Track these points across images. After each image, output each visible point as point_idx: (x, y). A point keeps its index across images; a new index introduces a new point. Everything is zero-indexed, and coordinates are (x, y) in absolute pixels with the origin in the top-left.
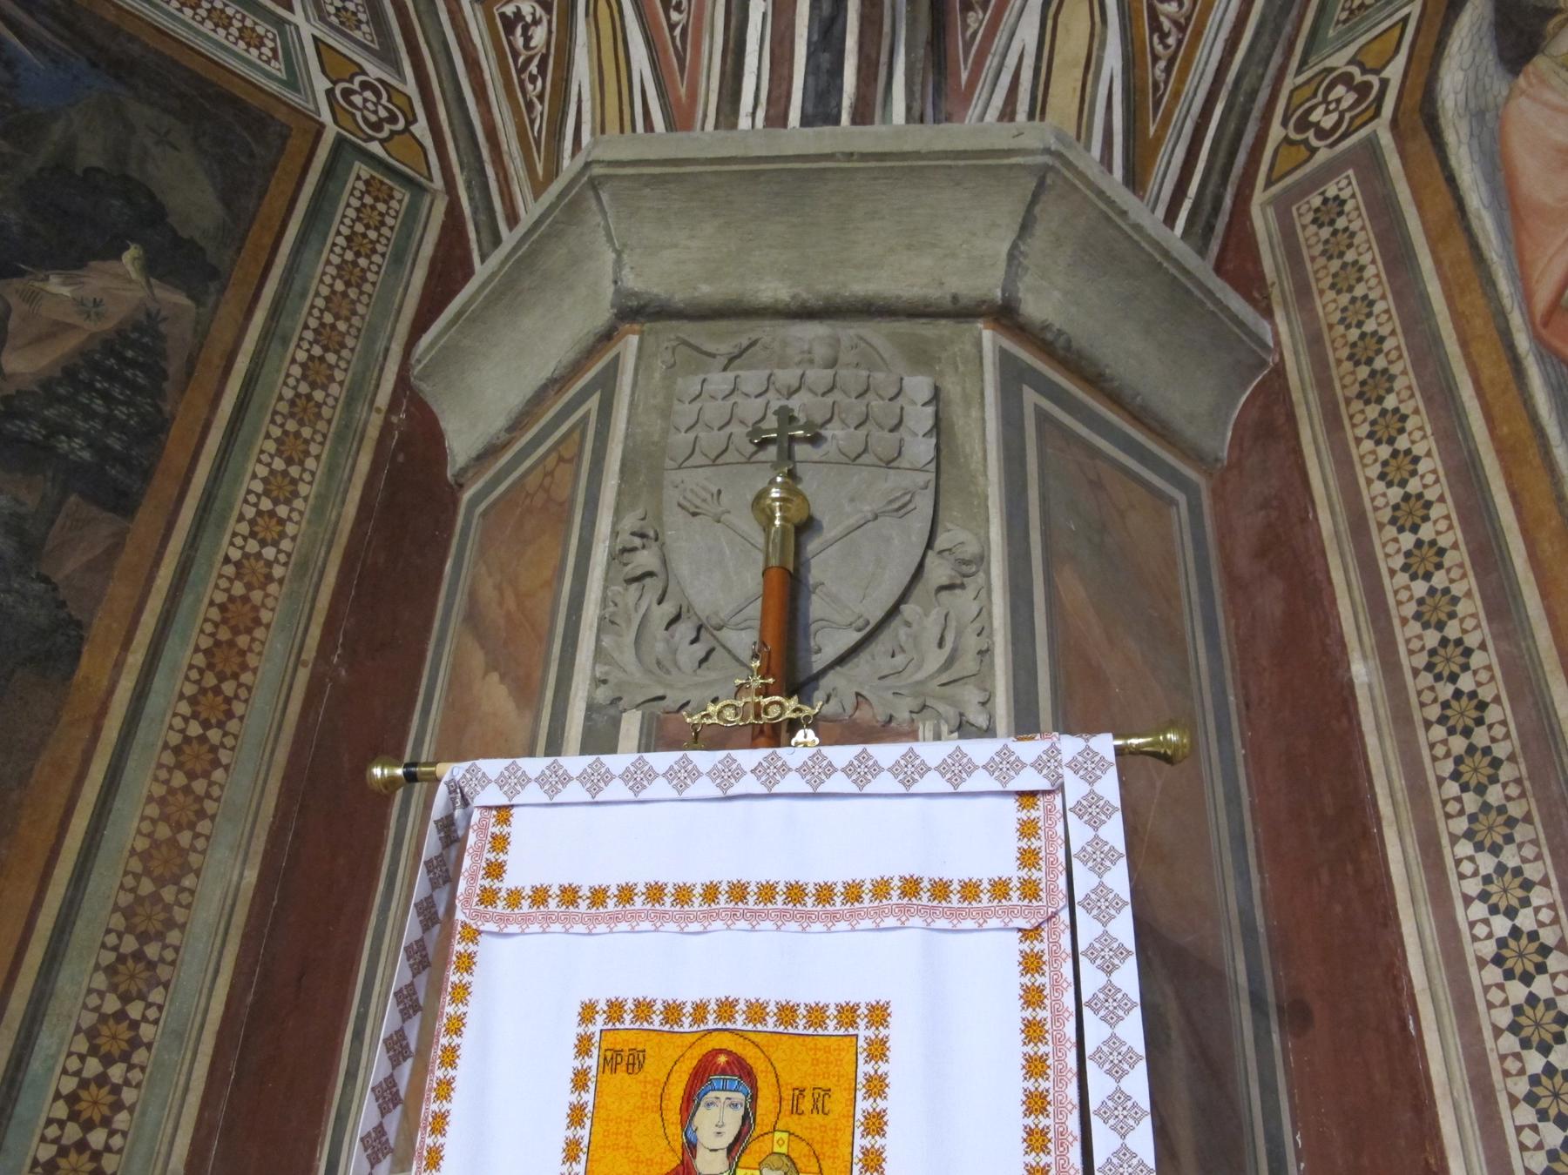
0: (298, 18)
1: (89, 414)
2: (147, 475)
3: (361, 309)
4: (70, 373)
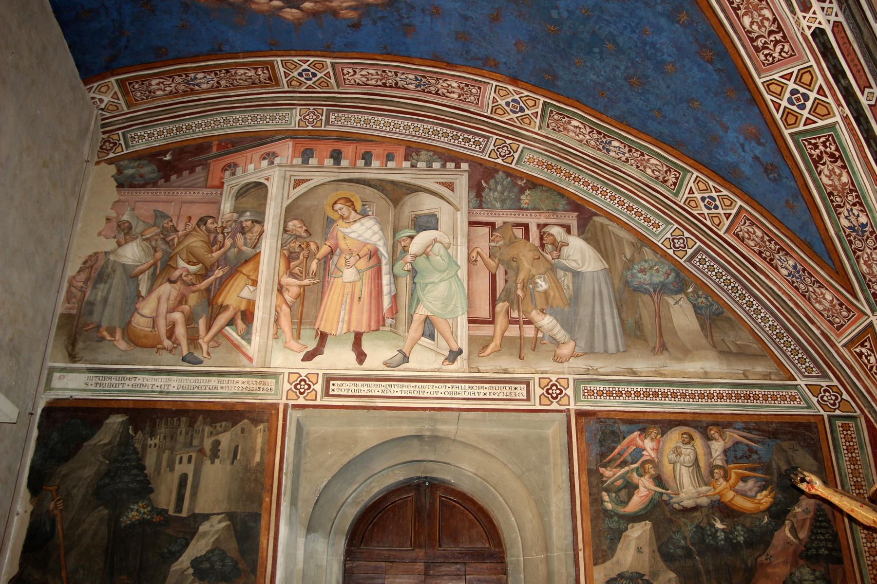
0: (799, 382)
1: (821, 541)
2: (841, 551)
3: (861, 471)
4: (812, 532)
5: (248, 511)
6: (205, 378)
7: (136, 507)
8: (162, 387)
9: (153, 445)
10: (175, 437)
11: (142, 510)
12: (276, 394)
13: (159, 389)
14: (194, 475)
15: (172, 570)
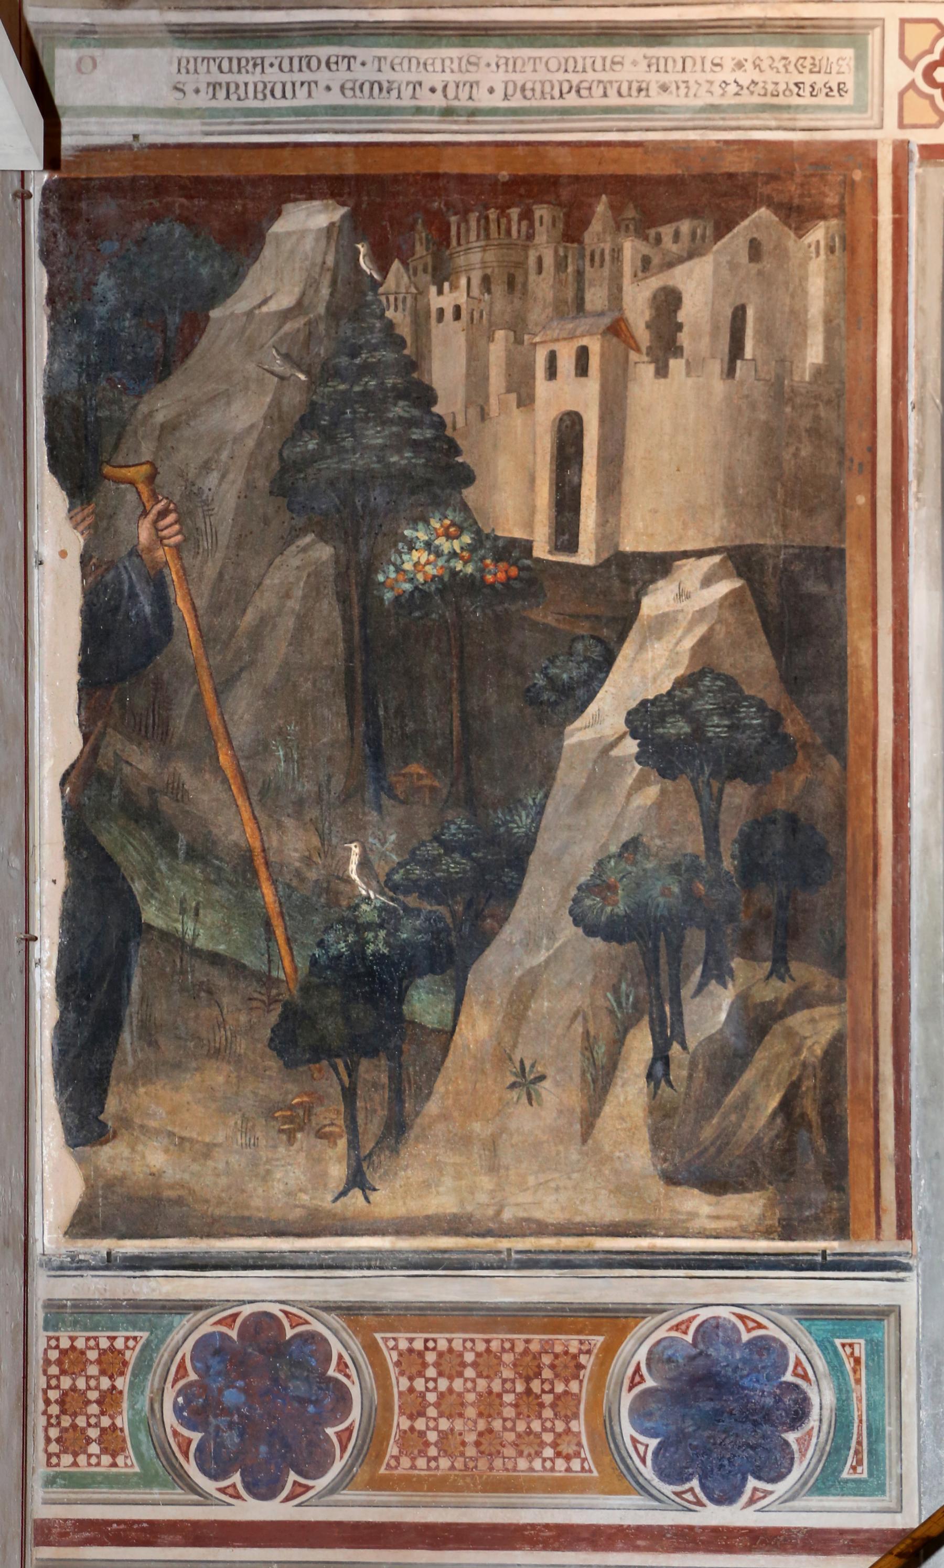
5: (798, 541)
6: (598, 52)
7: (422, 536)
8: (451, 92)
9: (449, 314)
10: (519, 279)
11: (445, 545)
12: (860, 107)
13: (438, 101)
14: (602, 420)
15: (566, 743)
